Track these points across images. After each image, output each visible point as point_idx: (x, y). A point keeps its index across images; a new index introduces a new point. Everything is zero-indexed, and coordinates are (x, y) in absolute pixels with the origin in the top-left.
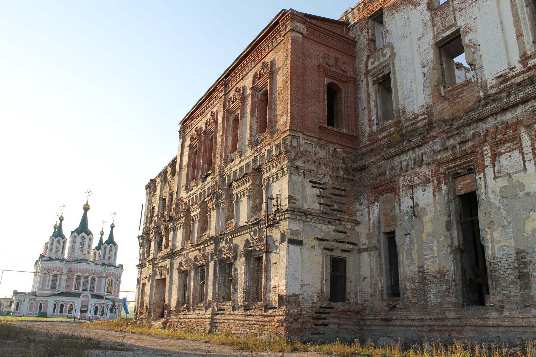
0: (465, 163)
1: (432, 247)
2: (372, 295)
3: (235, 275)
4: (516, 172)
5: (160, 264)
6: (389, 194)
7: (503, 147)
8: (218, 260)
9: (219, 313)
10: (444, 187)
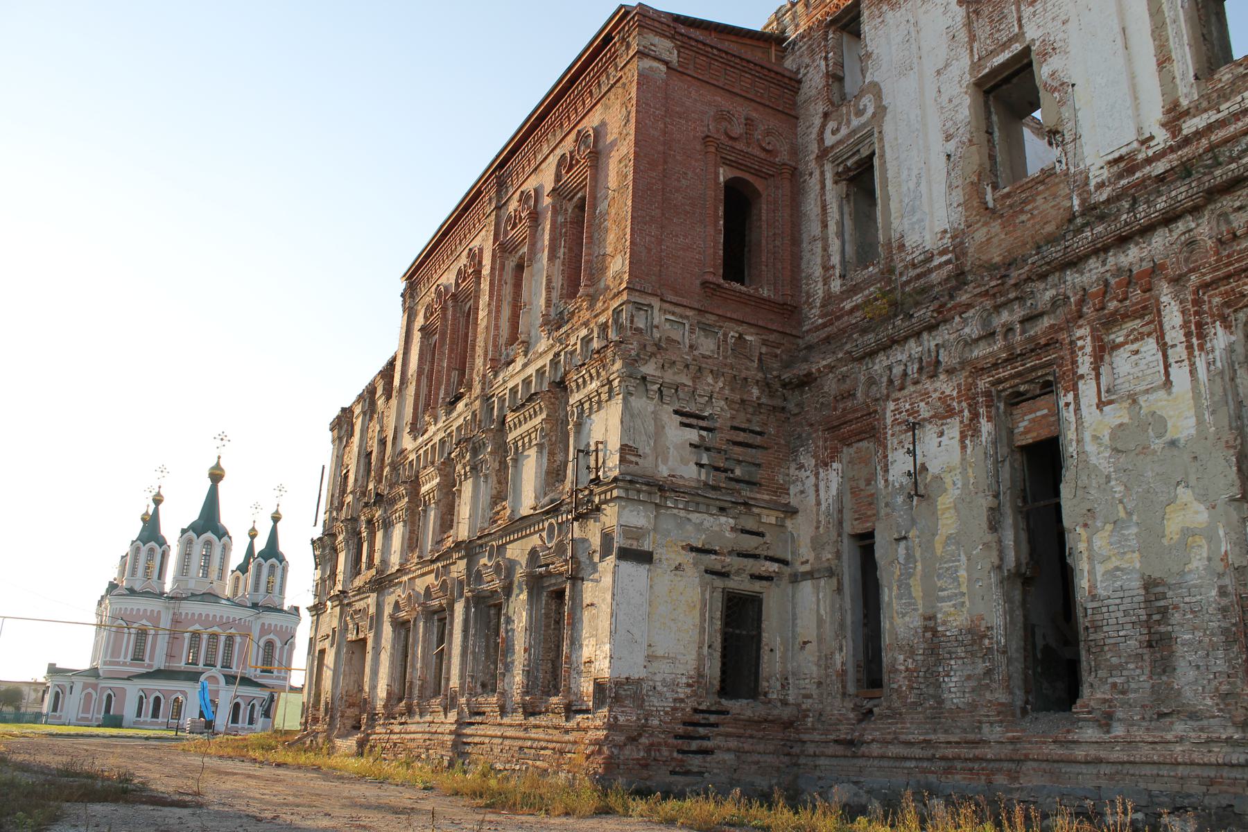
0: (1034, 369)
1: (956, 571)
2: (819, 684)
3: (507, 632)
4: (1147, 391)
5: (358, 606)
6: (864, 444)
7: (1121, 329)
8: (473, 596)
9: (472, 720)
10: (986, 427)
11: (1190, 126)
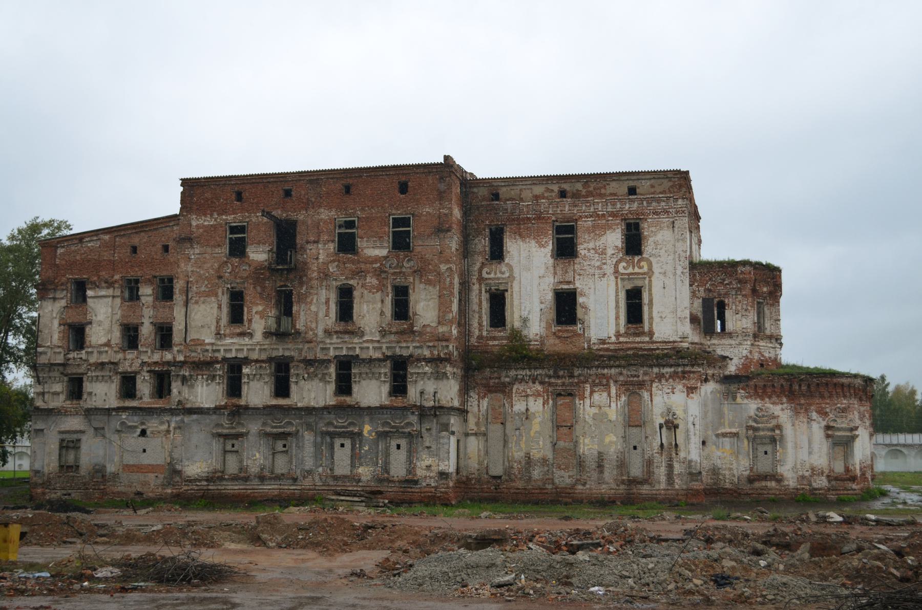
6: (499, 395)
10: (551, 402)
11: (621, 339)
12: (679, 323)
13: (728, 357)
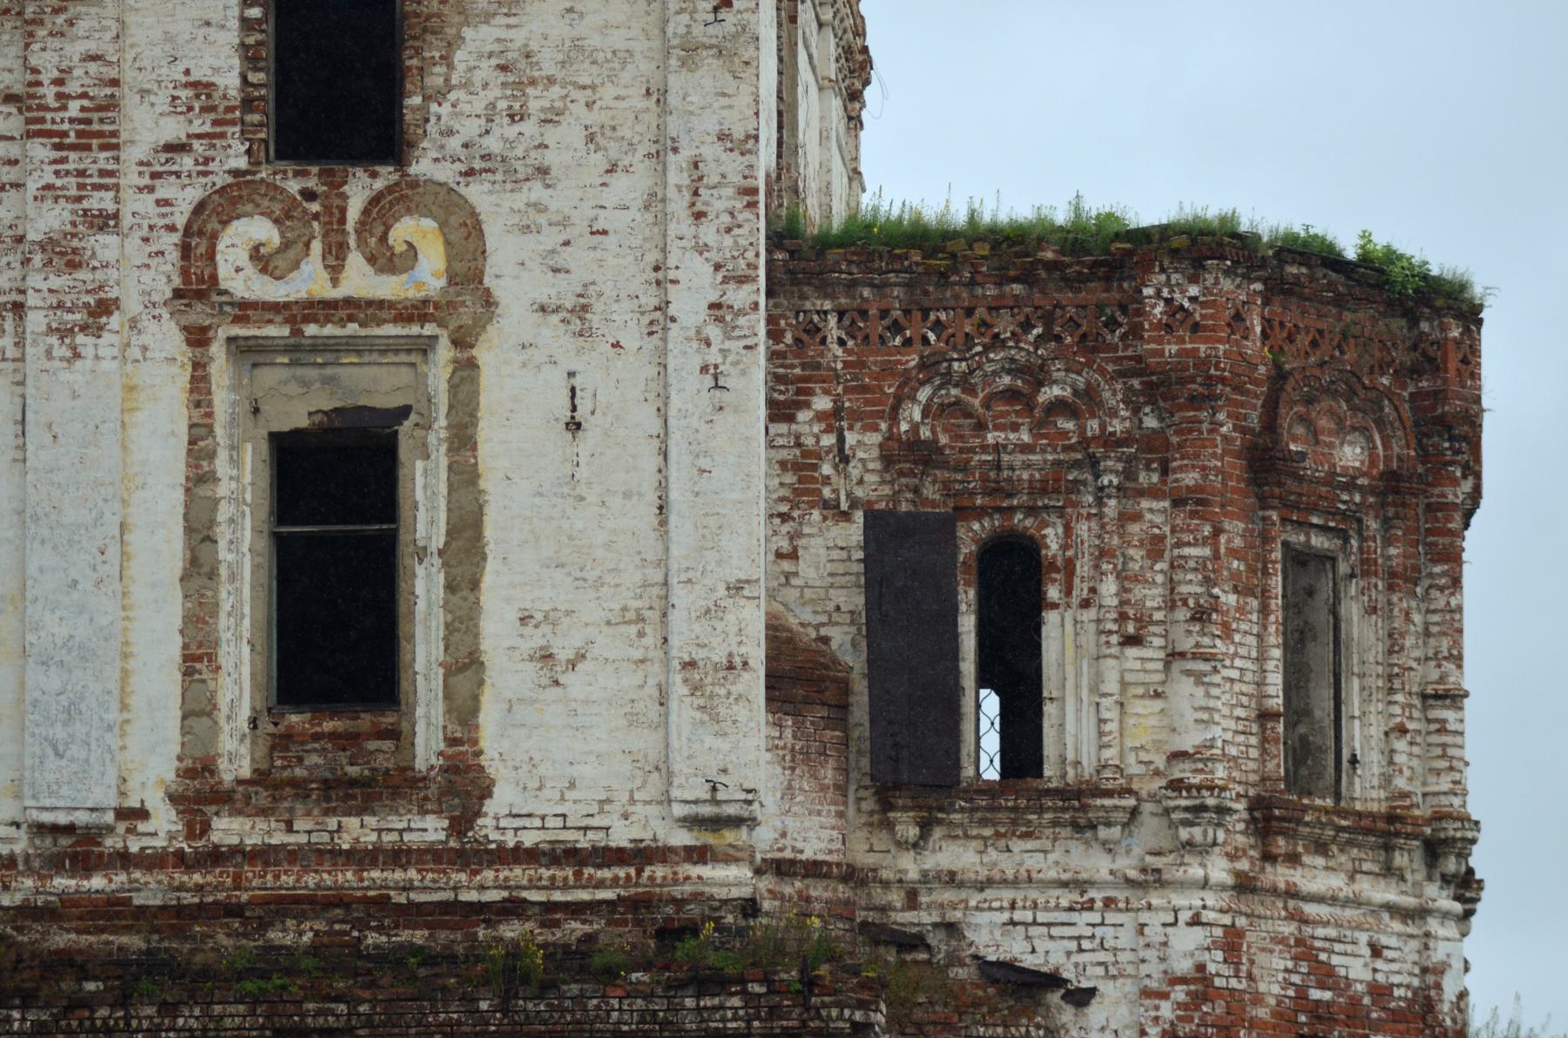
11: (227, 829)
12: (683, 711)
13: (1053, 980)
